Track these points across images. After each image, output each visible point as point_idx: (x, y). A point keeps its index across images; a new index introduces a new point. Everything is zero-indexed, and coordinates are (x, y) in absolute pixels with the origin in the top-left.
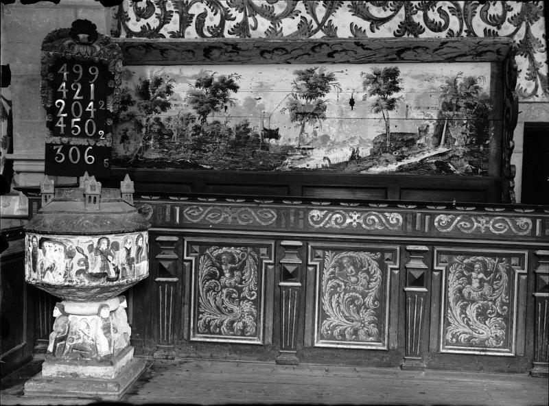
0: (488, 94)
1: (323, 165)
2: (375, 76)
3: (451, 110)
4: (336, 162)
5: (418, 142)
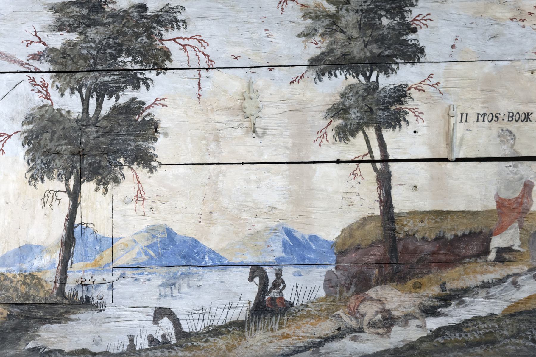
1: (152, 340)
4: (200, 327)
5: (497, 242)
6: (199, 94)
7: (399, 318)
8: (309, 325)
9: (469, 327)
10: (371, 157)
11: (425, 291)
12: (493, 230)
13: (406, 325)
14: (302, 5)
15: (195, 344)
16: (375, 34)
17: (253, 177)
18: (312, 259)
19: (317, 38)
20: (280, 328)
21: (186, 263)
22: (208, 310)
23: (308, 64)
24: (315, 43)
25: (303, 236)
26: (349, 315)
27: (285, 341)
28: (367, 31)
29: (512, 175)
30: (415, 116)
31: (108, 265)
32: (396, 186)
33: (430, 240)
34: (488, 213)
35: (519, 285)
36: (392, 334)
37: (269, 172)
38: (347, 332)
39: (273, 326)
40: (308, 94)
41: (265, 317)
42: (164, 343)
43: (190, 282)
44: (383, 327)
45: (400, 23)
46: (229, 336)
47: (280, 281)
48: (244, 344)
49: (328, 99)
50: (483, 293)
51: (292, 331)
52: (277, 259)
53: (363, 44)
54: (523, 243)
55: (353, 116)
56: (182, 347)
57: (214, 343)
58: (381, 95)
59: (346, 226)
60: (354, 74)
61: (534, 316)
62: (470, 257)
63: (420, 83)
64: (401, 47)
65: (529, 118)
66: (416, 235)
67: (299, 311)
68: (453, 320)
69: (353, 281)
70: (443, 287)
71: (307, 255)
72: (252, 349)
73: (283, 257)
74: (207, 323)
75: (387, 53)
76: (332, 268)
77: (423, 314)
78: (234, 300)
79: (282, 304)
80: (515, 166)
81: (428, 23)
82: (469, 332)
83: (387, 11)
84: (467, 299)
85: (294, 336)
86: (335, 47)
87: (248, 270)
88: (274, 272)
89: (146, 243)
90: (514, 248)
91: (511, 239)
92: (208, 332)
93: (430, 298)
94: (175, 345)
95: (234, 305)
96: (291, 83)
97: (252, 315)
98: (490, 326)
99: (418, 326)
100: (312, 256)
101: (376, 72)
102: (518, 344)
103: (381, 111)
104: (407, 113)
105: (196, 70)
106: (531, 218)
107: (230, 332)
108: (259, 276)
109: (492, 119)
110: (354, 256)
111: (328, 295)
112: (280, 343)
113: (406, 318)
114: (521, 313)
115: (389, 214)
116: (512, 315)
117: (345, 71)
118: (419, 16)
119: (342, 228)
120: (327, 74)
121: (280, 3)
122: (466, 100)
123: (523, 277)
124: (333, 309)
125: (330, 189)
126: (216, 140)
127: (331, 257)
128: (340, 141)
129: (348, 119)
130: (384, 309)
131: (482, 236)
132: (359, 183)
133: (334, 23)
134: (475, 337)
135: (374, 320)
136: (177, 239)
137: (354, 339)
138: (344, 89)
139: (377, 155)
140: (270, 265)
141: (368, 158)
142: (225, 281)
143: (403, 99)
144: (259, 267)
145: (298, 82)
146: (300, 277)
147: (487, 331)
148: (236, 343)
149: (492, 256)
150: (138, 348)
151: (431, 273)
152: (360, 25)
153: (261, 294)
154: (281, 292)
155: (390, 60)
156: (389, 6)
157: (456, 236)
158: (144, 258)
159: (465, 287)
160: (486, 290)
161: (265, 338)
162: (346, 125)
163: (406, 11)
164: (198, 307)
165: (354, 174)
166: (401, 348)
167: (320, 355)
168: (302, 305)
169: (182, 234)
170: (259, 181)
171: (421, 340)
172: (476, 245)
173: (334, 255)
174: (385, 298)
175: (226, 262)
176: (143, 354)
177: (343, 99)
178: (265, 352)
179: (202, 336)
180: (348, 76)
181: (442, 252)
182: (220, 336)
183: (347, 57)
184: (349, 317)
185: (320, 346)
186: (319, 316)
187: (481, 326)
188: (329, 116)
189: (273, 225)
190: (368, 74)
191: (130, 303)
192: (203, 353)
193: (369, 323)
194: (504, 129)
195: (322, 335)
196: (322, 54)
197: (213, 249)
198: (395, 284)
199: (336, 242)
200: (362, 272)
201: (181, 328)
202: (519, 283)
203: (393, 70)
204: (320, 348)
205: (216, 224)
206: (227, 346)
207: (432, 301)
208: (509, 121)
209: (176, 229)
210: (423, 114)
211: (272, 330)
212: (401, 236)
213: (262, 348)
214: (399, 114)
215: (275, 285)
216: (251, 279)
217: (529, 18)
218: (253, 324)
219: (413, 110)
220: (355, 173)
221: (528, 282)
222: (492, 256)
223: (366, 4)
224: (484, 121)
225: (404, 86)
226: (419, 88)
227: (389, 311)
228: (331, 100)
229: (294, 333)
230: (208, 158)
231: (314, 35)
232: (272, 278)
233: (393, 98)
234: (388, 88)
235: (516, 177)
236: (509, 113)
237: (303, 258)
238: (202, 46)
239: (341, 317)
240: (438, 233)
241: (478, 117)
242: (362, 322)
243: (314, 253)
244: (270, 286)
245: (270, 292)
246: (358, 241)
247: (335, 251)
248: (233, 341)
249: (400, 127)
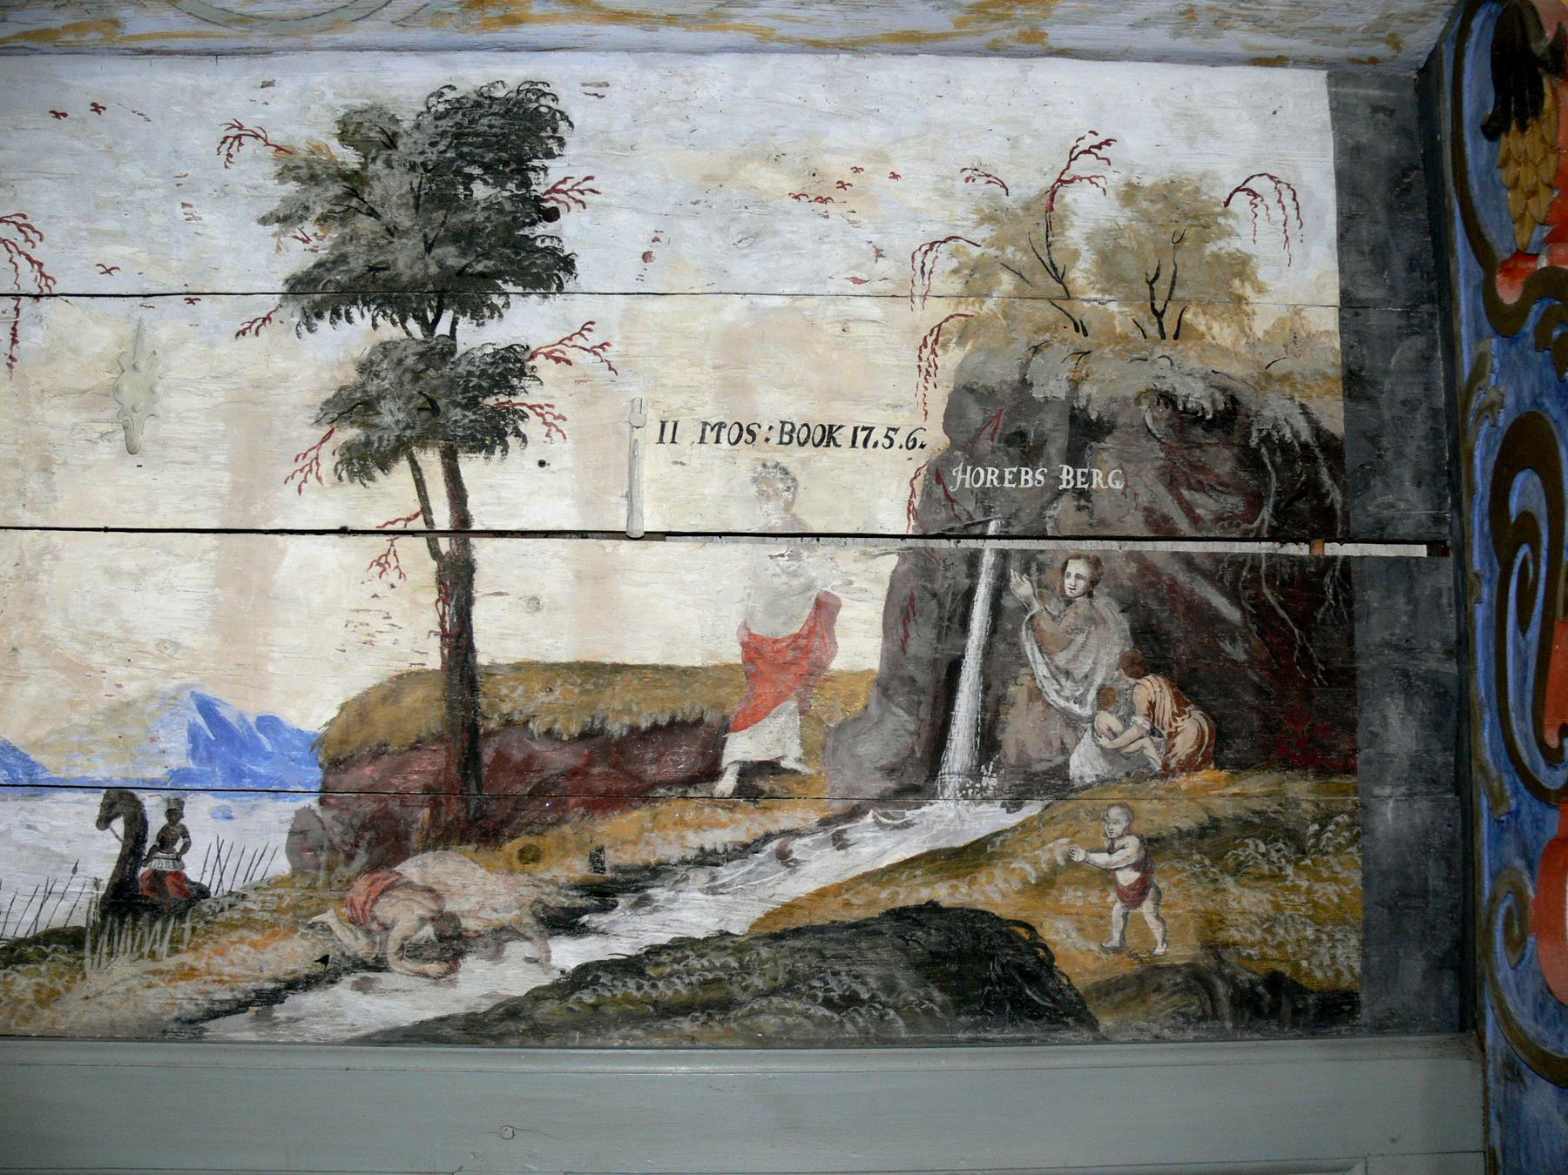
0: (1325, 321)
2: (350, 158)
3: (1024, 449)
5: (740, 748)
6: (11, 357)
7: (480, 936)
8: (246, 948)
9: (664, 964)
10: (426, 523)
11: (548, 870)
12: (732, 718)
13: (497, 955)
14: (279, 149)
16: (453, 220)
17: (128, 564)
18: (262, 776)
19: (310, 228)
20: (174, 951)
23: (284, 289)
24: (302, 240)
25: (242, 717)
26: (351, 926)
27: (185, 989)
28: (435, 215)
29: (784, 578)
30: (545, 423)
32: (488, 598)
33: (565, 738)
34: (717, 675)
35: (795, 861)
36: (460, 976)
37: (169, 553)
38: (345, 969)
39: (156, 947)
40: (279, 364)
41: (135, 920)
44: (439, 959)
45: (517, 196)
46: (43, 968)
48: (81, 989)
49: (326, 375)
50: (701, 877)
53: (422, 246)
54: (808, 754)
55: (387, 419)
58: (460, 370)
59: (353, 694)
60: (395, 316)
61: (831, 939)
62: (669, 784)
63: (560, 343)
64: (518, 254)
65: (834, 439)
66: (531, 725)
67: (222, 910)
68: (622, 947)
69: (363, 838)
70: (596, 860)
71: (248, 766)
72: (100, 1004)
73: (189, 769)
75: (480, 267)
76: (312, 802)
77: (542, 928)
78: (60, 875)
79: (181, 889)
80: (794, 556)
81: (588, 197)
82: (661, 977)
83: (487, 168)
84: (659, 893)
85: (210, 974)
86: (351, 248)
87: (97, 799)
88: (164, 808)
90: (784, 764)
91: (779, 740)
93: (561, 888)
95: (58, 888)
96: (238, 334)
97: (104, 915)
98: (718, 964)
99: (529, 960)
101: (451, 312)
102: (787, 1012)
103: (458, 410)
104: (524, 416)
105: (8, 299)
106: (831, 688)
107: (45, 956)
108: (125, 814)
109: (740, 436)
110: (367, 773)
111: (297, 870)
112: (172, 990)
113: (502, 935)
114: (797, 932)
115: (463, 669)
116: (777, 937)
117: (373, 307)
118: (564, 181)
119: (341, 701)
120: (327, 315)
121: (223, 143)
122: (677, 389)
123: (807, 840)
124: (309, 908)
125: (317, 600)
126: (45, 470)
127: (311, 772)
128: (352, 481)
129: (375, 426)
130: (440, 911)
131: (701, 732)
132: (393, 586)
133: (353, 193)
134: (677, 991)
135: (414, 939)
137: (363, 987)
138: (367, 351)
139: (443, 518)
140: (153, 787)
141: (419, 524)
142: (38, 825)
143: (515, 381)
145: (257, 333)
147: (710, 976)
149: (727, 783)
151: (566, 822)
152: (417, 198)
153: (126, 862)
154: (178, 859)
155: (487, 279)
156: (491, 155)
157: (634, 729)
159: (653, 861)
160: (708, 869)
161: (134, 977)
162: (368, 443)
163: (534, 169)
165: (381, 563)
166: (485, 1014)
167: (275, 1024)
170: (139, 576)
171: (537, 996)
172: (687, 753)
174: (446, 885)
175: (45, 776)
177: (365, 377)
178: (134, 1012)
180: (380, 320)
181: (596, 770)
182: (19, 967)
183: (381, 274)
184: (351, 930)
185: (275, 1003)
186: (272, 925)
187: (695, 963)
188: (328, 418)
189: (169, 686)
190: (430, 316)
193: (402, 948)
194: (768, 464)
195: (281, 975)
196: (319, 265)
198: (471, 848)
199: (325, 735)
200: (386, 815)
202: (794, 856)
203: (494, 309)
204: (275, 1006)
205: (25, 678)
206: (39, 992)
207: (566, 896)
208: (781, 443)
210: (565, 419)
212: (492, 725)
214: (504, 418)
215: (164, 842)
216: (104, 822)
217: (839, 195)
218: (106, 938)
219: (539, 410)
220: (383, 561)
221: (818, 853)
222: (727, 783)
223: (435, 150)
224: (718, 441)
225: (518, 349)
226: (557, 354)
227: (453, 918)
228: (333, 378)
229: (208, 965)
230: (19, 514)
231: (302, 219)
232: (156, 821)
233: (491, 377)
234: (480, 354)
235: (795, 582)
236: (783, 423)
237: (237, 773)
238: (27, 240)
239: (329, 930)
240: (589, 720)
241: (704, 431)
242: (383, 944)
243: (267, 763)
245: (149, 858)
246: (381, 735)
247: (321, 759)
248: (52, 981)
249: (505, 450)
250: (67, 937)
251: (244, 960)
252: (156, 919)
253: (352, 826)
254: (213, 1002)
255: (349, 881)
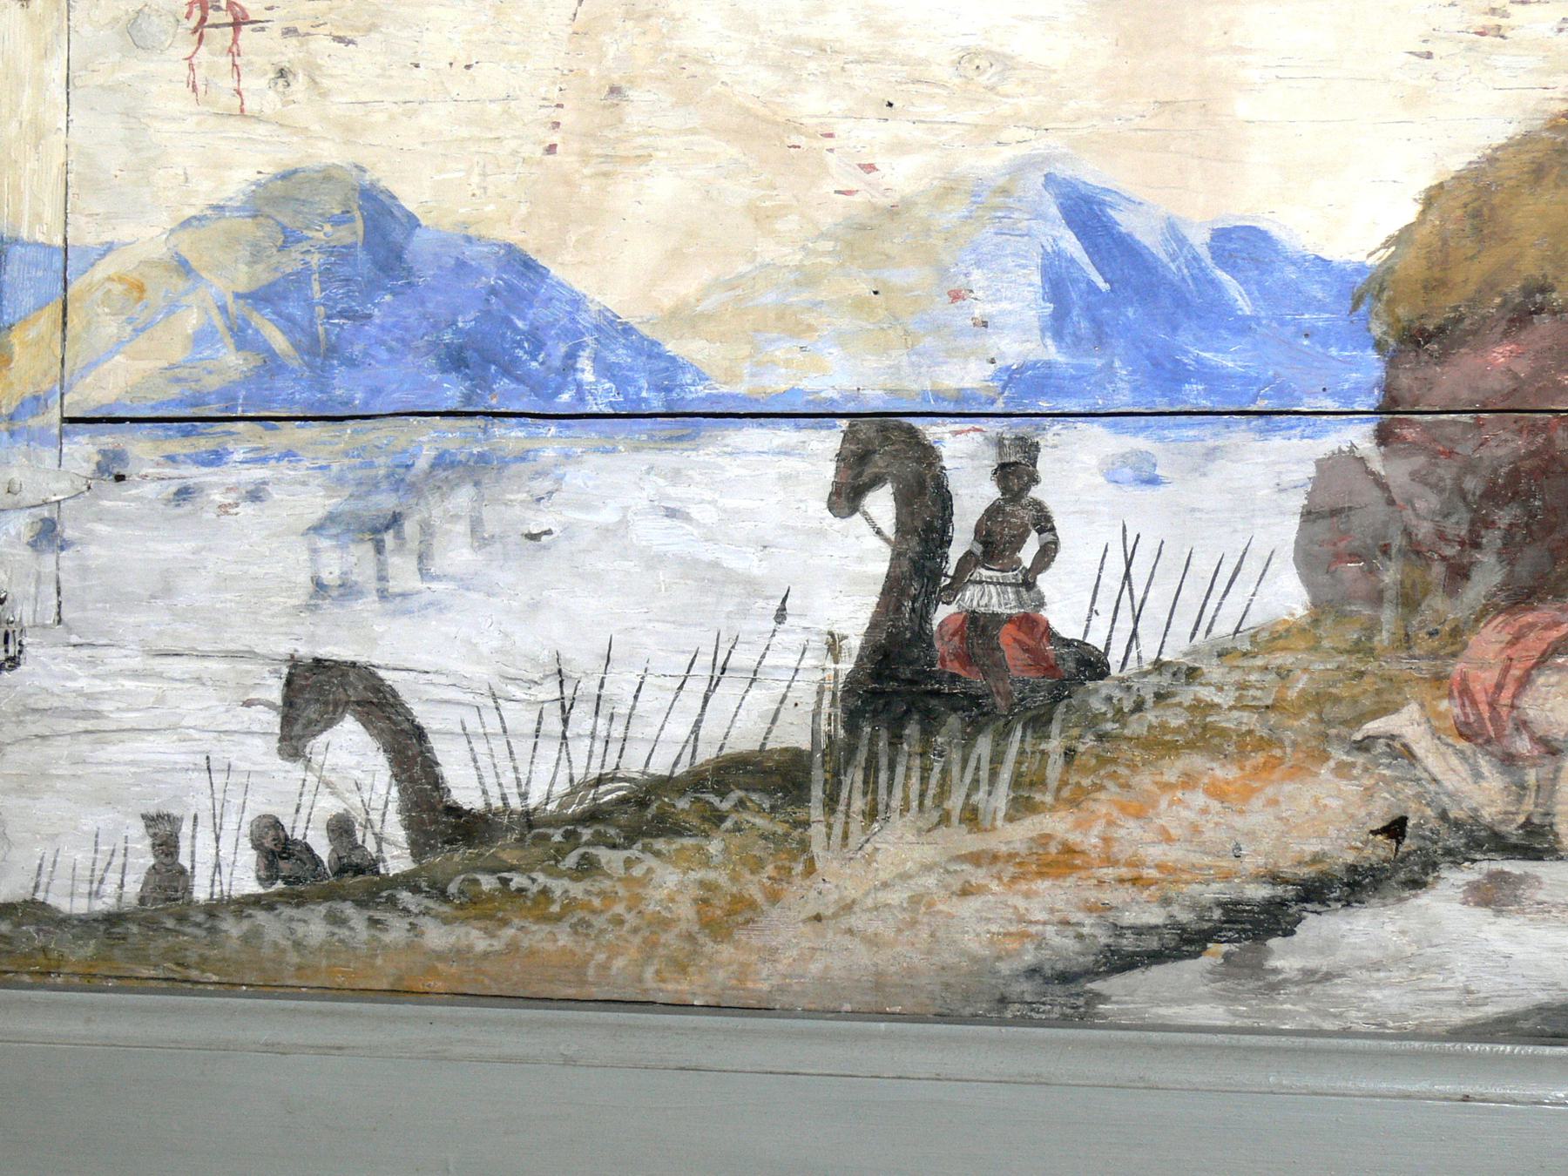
8: (1199, 799)
15: (517, 880)
18: (1230, 377)
20: (1022, 806)
21: (468, 399)
22: (590, 686)
26: (1463, 744)
31: (37, 403)
38: (1449, 852)
39: (980, 797)
41: (927, 732)
42: (342, 869)
43: (487, 513)
46: (714, 847)
47: (1027, 515)
48: (803, 898)
51: (1098, 828)
52: (1012, 377)
56: (443, 896)
57: (628, 881)
67: (1139, 707)
69: (1490, 525)
71: (1197, 350)
72: (850, 931)
73: (1048, 365)
74: (583, 762)
76: (1359, 436)
78: (746, 626)
79: (1037, 657)
85: (1111, 861)
87: (827, 443)
88: (990, 460)
89: (243, 277)
92: (593, 816)
94: (407, 881)
95: (743, 658)
97: (852, 726)
100: (1229, 359)
107: (720, 818)
108: (896, 479)
111: (1325, 607)
112: (1021, 903)
119: (1428, 180)
124: (1355, 701)
127: (1350, 364)
136: (419, 246)
140: (963, 412)
142: (694, 511)
144: (899, 427)
146: (1149, 492)
148: (753, 888)
150: (201, 893)
153: (903, 592)
154: (1028, 584)
158: (232, 362)
161: (928, 868)
164: (534, 661)
167: (1274, 987)
168: (1159, 665)
169: (446, 224)
173: (1373, 355)
175: (701, 390)
176: (232, 928)
178: (929, 952)
179: (557, 837)
182: (660, 844)
184: (1461, 754)
185: (1272, 933)
189: (990, 162)
191: (152, 622)
192: (564, 939)
195: (1286, 867)
197: (630, 313)
199: (1388, 269)
201: (437, 782)
204: (1274, 943)
205: (644, 159)
206: (705, 901)
209: (411, 195)
211: (972, 817)
213: (913, 923)
218: (859, 776)
229: (1106, 840)
237: (1168, 371)
239: (1408, 754)
243: (1245, 343)
244: (961, 541)
245: (958, 583)
246: (1530, 267)
247: (1377, 330)
248: (734, 879)
250: (767, 772)
251: (1196, 829)
252: (979, 730)
253: (1463, 495)
254: (1118, 930)
255: (1456, 632)
